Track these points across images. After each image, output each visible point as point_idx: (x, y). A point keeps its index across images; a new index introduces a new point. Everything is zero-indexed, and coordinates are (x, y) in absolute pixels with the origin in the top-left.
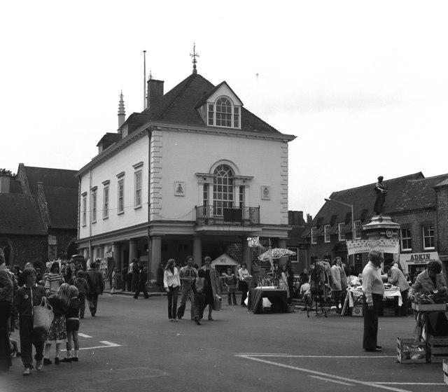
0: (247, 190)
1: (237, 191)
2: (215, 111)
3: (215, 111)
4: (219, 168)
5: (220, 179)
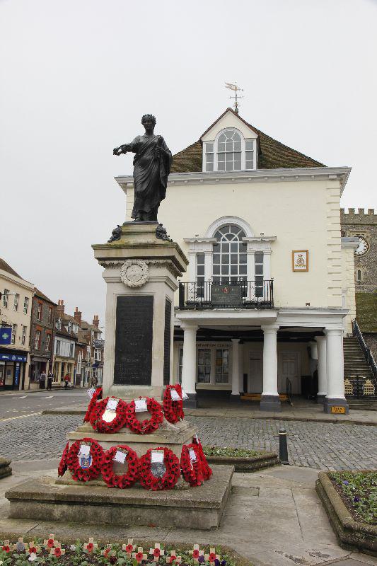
0: (266, 257)
1: (251, 261)
2: (215, 150)
3: (215, 150)
4: (224, 228)
5: (226, 248)
